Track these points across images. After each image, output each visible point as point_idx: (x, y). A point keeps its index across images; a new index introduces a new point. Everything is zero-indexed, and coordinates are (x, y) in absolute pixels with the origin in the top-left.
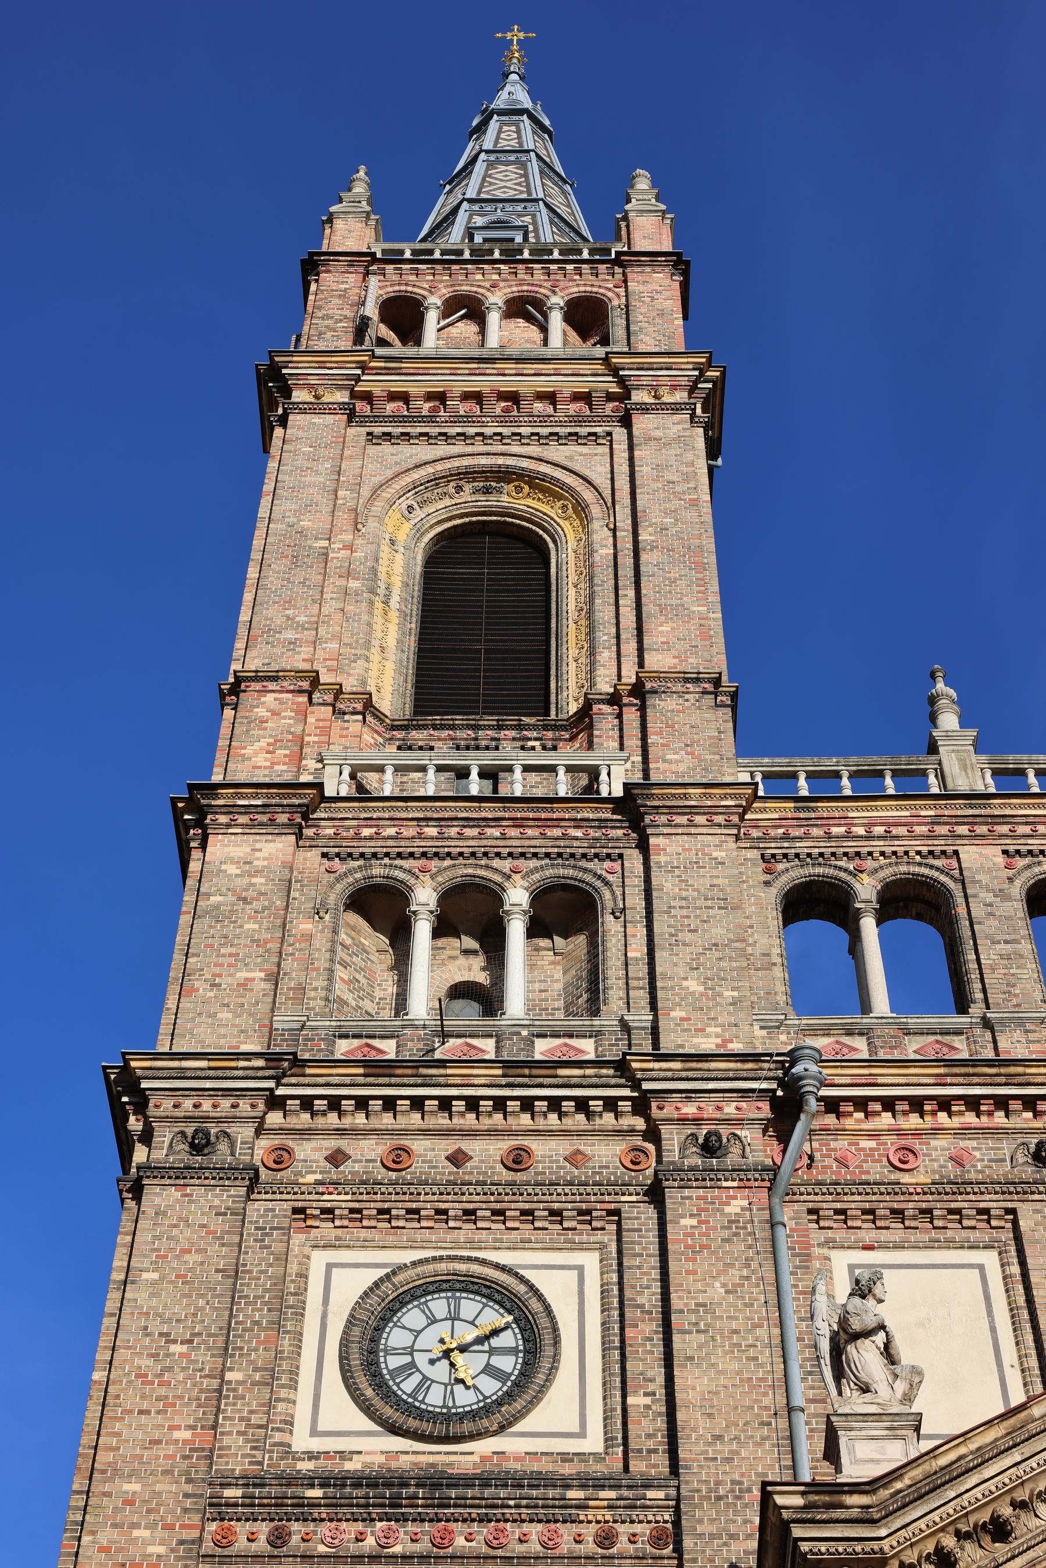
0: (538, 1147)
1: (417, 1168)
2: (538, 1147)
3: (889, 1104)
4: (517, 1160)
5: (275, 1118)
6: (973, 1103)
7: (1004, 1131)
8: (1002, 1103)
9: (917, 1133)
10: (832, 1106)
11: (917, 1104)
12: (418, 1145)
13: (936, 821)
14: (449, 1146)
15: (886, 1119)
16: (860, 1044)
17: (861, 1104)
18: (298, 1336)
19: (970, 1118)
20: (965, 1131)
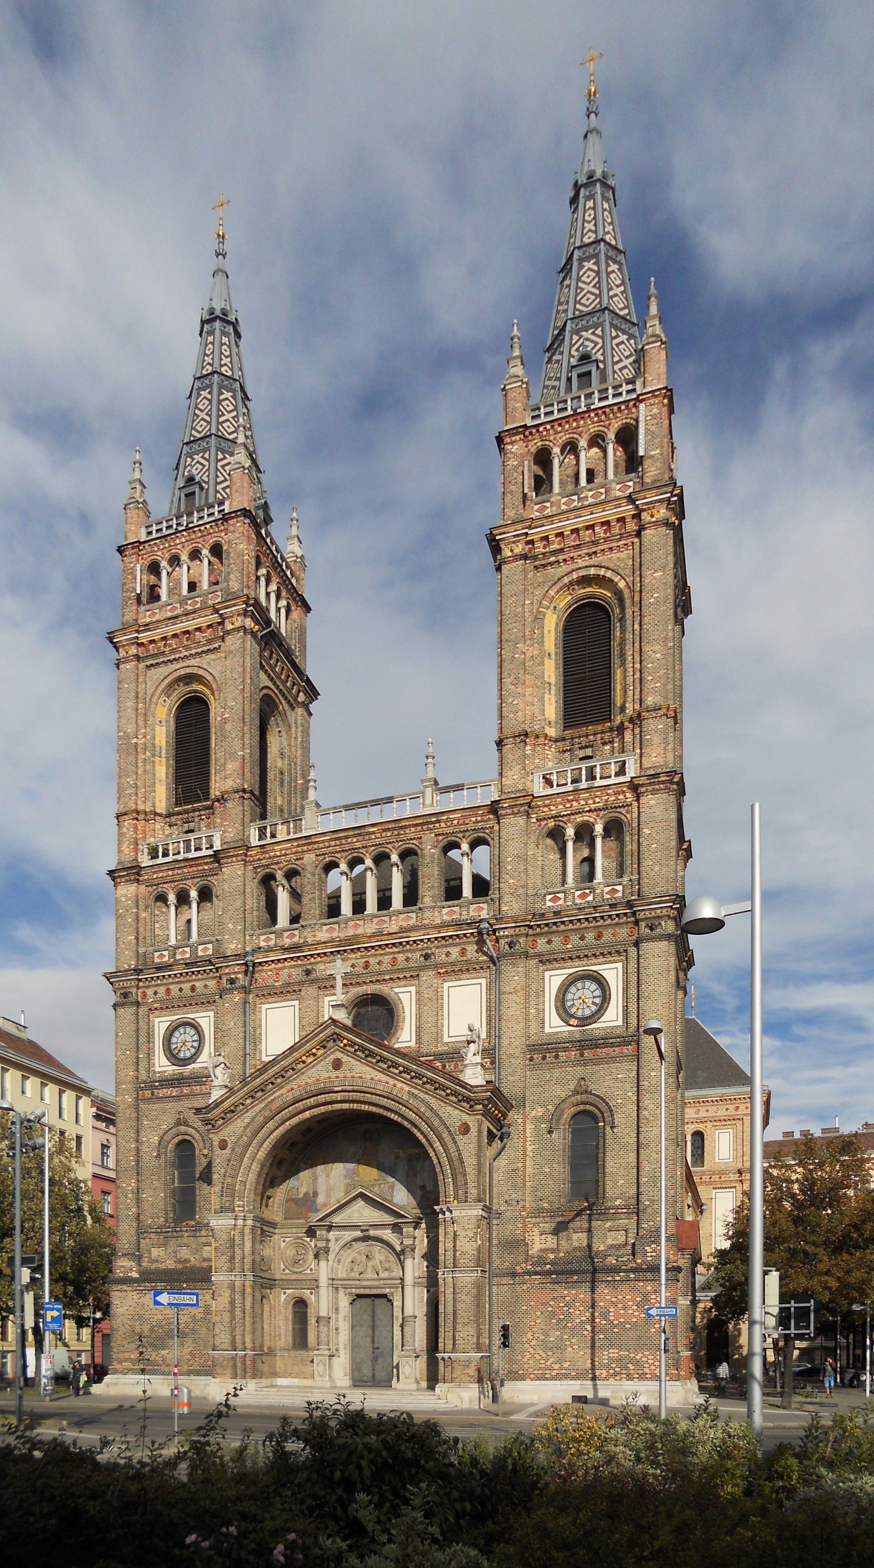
0: (197, 984)
1: (173, 994)
2: (197, 984)
3: (272, 961)
4: (193, 989)
5: (141, 984)
6: (292, 958)
7: (300, 966)
8: (298, 957)
9: (281, 969)
10: (260, 963)
11: (279, 960)
12: (172, 987)
13: (298, 846)
14: (178, 986)
15: (273, 966)
16: (273, 936)
17: (266, 962)
19: (293, 963)
20: (291, 967)
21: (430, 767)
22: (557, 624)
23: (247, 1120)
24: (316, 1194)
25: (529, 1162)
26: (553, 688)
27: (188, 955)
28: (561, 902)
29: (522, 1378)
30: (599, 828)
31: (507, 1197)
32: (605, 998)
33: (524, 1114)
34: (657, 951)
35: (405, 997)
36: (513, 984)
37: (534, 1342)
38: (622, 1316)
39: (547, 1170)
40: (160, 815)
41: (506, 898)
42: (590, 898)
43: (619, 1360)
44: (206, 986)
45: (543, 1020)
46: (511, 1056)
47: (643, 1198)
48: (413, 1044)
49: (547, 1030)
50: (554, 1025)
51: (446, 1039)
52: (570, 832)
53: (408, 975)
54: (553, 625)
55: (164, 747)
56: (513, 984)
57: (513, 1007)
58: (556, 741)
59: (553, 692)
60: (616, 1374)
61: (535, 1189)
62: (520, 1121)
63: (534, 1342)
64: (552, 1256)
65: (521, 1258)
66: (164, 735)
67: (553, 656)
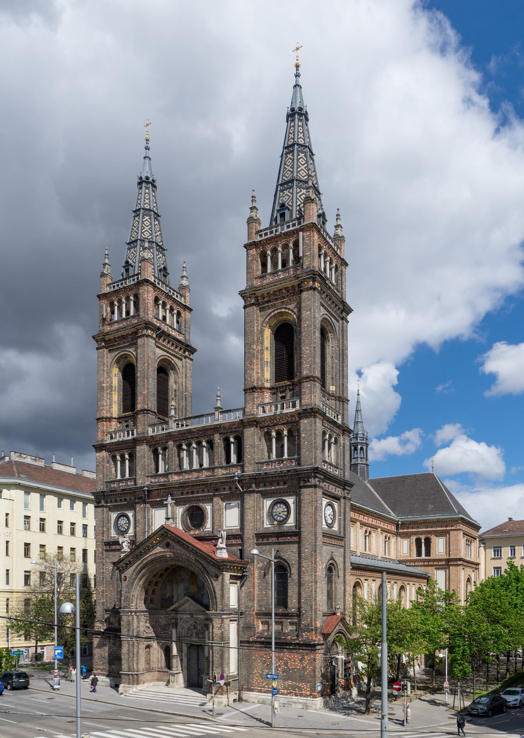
8: (165, 489)
18: (111, 523)
21: (219, 402)
23: (134, 568)
24: (173, 597)
25: (256, 588)
27: (124, 484)
28: (270, 467)
29: (252, 690)
30: (285, 432)
31: (247, 604)
32: (289, 512)
33: (254, 566)
34: (308, 492)
35: (208, 508)
36: (249, 505)
37: (257, 674)
38: (293, 665)
39: (264, 593)
41: (247, 465)
42: (282, 465)
43: (292, 686)
44: (130, 499)
45: (263, 521)
46: (249, 538)
47: (302, 609)
48: (211, 529)
49: (265, 526)
50: (267, 525)
52: (274, 434)
53: (209, 498)
56: (249, 505)
57: (249, 517)
58: (270, 389)
59: (269, 366)
60: (290, 693)
61: (259, 601)
62: (252, 569)
63: (257, 674)
64: (266, 634)
65: (252, 634)
67: (269, 349)
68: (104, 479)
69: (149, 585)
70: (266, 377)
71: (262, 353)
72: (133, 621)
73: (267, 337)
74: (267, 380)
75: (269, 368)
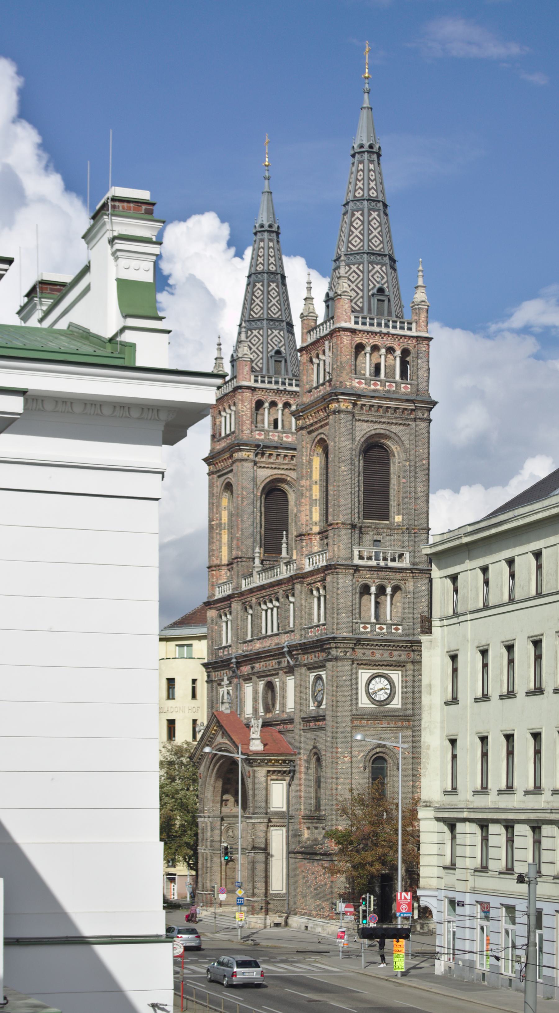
22: (321, 462)
26: (318, 502)
40: (224, 565)
51: (288, 711)
54: (318, 463)
55: (227, 523)
59: (318, 504)
66: (226, 516)
67: (318, 482)
68: (212, 646)
69: (224, 784)
70: (314, 519)
71: (311, 490)
72: (206, 829)
73: (316, 468)
74: (316, 523)
75: (318, 508)
